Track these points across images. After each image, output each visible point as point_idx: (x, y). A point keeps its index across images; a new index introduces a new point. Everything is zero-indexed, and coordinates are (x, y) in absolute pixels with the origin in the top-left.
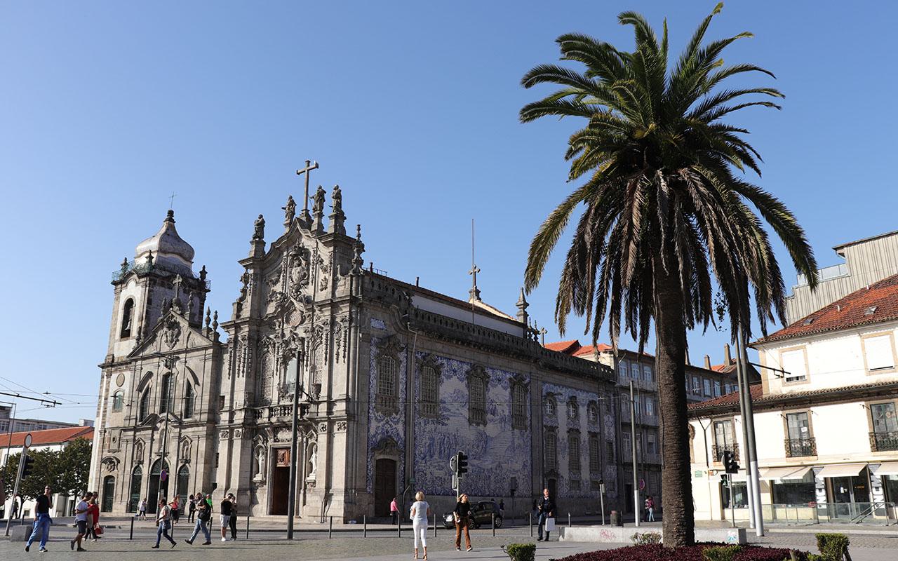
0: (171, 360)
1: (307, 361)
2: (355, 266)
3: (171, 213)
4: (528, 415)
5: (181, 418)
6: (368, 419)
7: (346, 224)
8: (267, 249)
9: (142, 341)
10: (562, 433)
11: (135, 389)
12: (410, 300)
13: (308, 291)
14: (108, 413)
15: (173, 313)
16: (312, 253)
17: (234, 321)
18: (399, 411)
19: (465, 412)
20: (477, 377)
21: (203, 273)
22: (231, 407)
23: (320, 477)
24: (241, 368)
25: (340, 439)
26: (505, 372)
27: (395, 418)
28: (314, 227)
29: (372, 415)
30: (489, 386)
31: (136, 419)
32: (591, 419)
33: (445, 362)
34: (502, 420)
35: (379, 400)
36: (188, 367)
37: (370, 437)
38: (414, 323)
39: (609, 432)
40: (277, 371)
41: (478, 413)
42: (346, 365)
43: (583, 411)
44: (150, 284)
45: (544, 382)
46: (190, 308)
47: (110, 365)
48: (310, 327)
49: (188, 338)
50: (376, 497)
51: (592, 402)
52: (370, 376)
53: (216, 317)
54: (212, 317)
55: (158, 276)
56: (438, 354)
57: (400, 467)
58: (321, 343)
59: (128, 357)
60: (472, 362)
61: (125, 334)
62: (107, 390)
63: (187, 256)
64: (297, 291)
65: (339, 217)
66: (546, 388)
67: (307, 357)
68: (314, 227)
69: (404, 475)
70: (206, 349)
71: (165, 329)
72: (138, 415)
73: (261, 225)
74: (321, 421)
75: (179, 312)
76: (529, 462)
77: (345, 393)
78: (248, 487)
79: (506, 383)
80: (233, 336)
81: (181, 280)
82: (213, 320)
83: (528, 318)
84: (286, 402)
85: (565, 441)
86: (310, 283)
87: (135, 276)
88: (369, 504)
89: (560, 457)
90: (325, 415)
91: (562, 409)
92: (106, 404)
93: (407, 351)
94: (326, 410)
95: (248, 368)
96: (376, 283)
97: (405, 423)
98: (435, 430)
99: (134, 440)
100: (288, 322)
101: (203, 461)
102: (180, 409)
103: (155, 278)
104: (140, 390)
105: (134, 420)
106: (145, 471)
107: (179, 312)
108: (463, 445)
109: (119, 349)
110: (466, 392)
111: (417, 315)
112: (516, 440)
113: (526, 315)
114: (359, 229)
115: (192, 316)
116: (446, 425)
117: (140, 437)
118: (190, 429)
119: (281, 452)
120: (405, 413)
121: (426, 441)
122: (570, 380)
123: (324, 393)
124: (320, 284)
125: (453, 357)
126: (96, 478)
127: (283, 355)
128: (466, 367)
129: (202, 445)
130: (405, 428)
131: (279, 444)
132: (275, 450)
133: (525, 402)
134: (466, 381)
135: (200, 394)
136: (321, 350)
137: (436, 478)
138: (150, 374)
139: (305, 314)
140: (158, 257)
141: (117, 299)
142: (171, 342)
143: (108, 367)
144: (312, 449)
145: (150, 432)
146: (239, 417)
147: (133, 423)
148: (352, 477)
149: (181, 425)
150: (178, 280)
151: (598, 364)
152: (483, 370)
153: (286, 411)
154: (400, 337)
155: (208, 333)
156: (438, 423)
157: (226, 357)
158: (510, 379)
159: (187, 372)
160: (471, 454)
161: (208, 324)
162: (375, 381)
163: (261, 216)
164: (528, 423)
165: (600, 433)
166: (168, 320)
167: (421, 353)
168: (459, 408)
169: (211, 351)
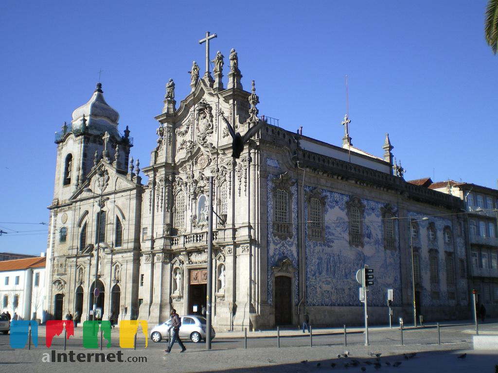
0: (103, 200)
2: (251, 115)
3: (100, 85)
4: (397, 238)
5: (112, 247)
6: (268, 243)
7: (242, 81)
9: (80, 186)
10: (424, 253)
12: (298, 143)
13: (212, 139)
15: (103, 163)
16: (214, 107)
17: (153, 166)
18: (293, 235)
19: (346, 236)
20: (354, 206)
21: (127, 132)
22: (152, 237)
23: (228, 292)
24: (160, 205)
25: (244, 261)
26: (377, 202)
27: (289, 241)
28: (216, 85)
29: (271, 239)
30: (365, 214)
31: (78, 248)
32: (447, 241)
33: (328, 194)
34: (377, 242)
35: (276, 226)
36: (117, 206)
37: (270, 257)
38: (302, 162)
39: (461, 251)
40: (189, 205)
41: (357, 237)
42: (248, 198)
43: (440, 234)
45: (409, 211)
46: (117, 159)
47: (57, 207)
48: (216, 168)
49: (116, 182)
50: (276, 307)
51: (446, 228)
52: (268, 206)
53: (138, 165)
54: (135, 163)
55: (90, 135)
56: (323, 188)
57: (295, 283)
58: (225, 180)
59: (69, 200)
60: (350, 194)
61: (67, 182)
62: (55, 227)
63: (113, 118)
64: (204, 139)
65: (237, 74)
66: (410, 216)
67: (214, 192)
68: (216, 85)
69: (298, 289)
70: (131, 190)
71: (97, 176)
74: (228, 245)
75: (108, 162)
76: (399, 277)
77: (248, 221)
79: (378, 211)
80: (152, 179)
81: (109, 136)
83: (393, 158)
84: (198, 231)
85: (427, 259)
86: (214, 132)
87: (73, 136)
88: (270, 314)
89: (423, 273)
90: (231, 240)
91: (423, 232)
92: (54, 238)
93: (297, 185)
94: (232, 236)
96: (270, 129)
97: (298, 246)
98: (323, 251)
99: (77, 265)
100: (196, 162)
102: (111, 239)
104: (80, 226)
105: (76, 250)
106: (86, 291)
107: (108, 162)
108: (345, 263)
109: (62, 194)
110: (346, 219)
111: (304, 156)
112: (388, 258)
113: (391, 156)
114: (254, 85)
115: (119, 164)
116: (331, 247)
117: (81, 263)
118: (120, 255)
119: (194, 273)
120: (298, 237)
121: (315, 260)
122: (429, 208)
123: (229, 221)
124: (222, 132)
125: (335, 190)
126: (49, 296)
127: (194, 192)
128: (345, 199)
129: (130, 266)
130: (298, 250)
131: (194, 266)
132: (190, 270)
133: (394, 227)
134: (346, 210)
135: (127, 226)
136: (226, 186)
137: (325, 291)
138: (87, 212)
139: (211, 157)
140: (91, 120)
141: (60, 154)
142: (103, 186)
143: (54, 208)
144: (220, 268)
145: (89, 258)
146: (159, 244)
147: (75, 252)
148: (255, 292)
149: (113, 252)
150: (107, 136)
151: (449, 196)
152: (359, 201)
153: (198, 238)
154: (292, 174)
155: (132, 177)
156: (324, 245)
157: (146, 196)
158: (382, 208)
159: (116, 209)
160: (352, 271)
161: (132, 170)
162: (272, 211)
164: (397, 244)
165: (454, 253)
166: (99, 169)
167: (309, 187)
168: (342, 233)
169: (135, 192)
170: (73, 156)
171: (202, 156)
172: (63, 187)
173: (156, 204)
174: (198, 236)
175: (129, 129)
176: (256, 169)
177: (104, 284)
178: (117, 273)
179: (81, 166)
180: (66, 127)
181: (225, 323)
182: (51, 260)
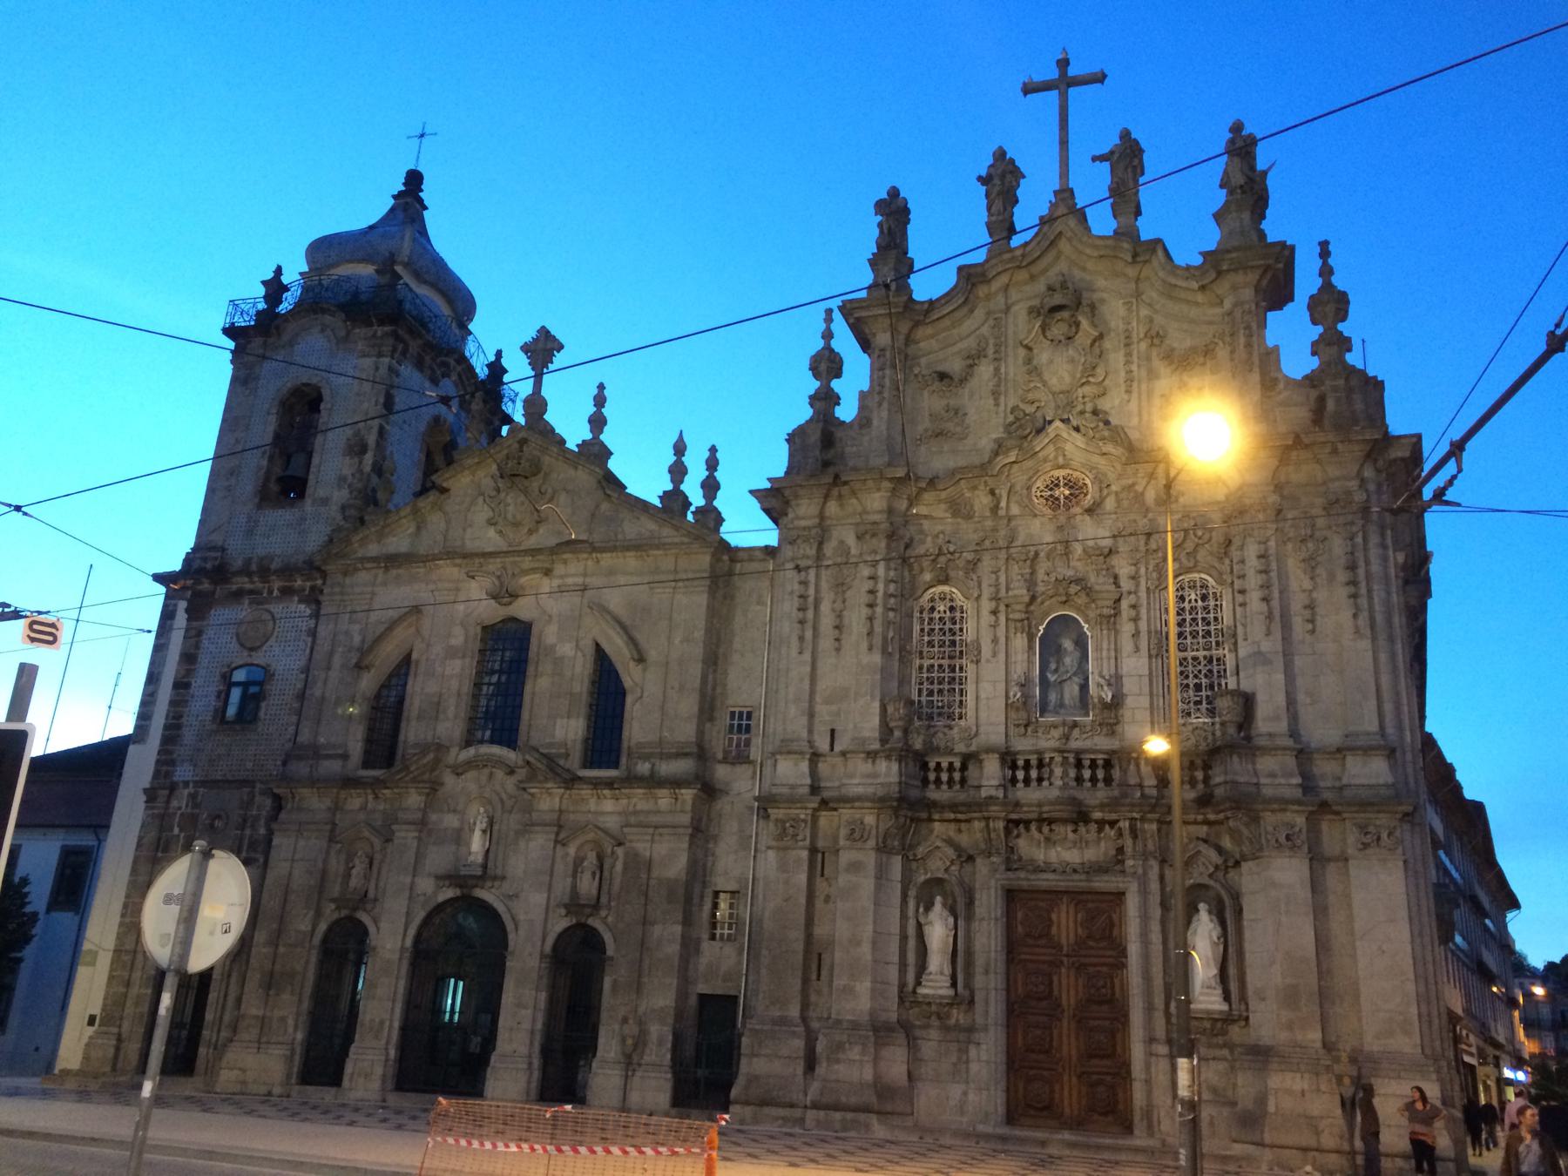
1: (1136, 620)
8: (927, 286)
11: (337, 661)
14: (188, 736)
40: (995, 641)
44: (394, 350)
53: (712, 464)
62: (189, 658)
72: (356, 748)
73: (894, 212)
78: (894, 1017)
82: (696, 473)
95: (888, 624)
101: (680, 918)
103: (407, 337)
109: (250, 532)
126: (117, 952)
132: (1011, 896)
147: (331, 767)
153: (1087, 774)
163: (894, 193)
170: (326, 393)
171: (1060, 473)
172: (259, 507)
173: (827, 621)
174: (1087, 763)
175: (505, 362)
176: (1389, 541)
177: (506, 918)
178: (587, 876)
179: (372, 439)
180: (275, 288)
181: (1307, 1139)
182: (151, 795)
